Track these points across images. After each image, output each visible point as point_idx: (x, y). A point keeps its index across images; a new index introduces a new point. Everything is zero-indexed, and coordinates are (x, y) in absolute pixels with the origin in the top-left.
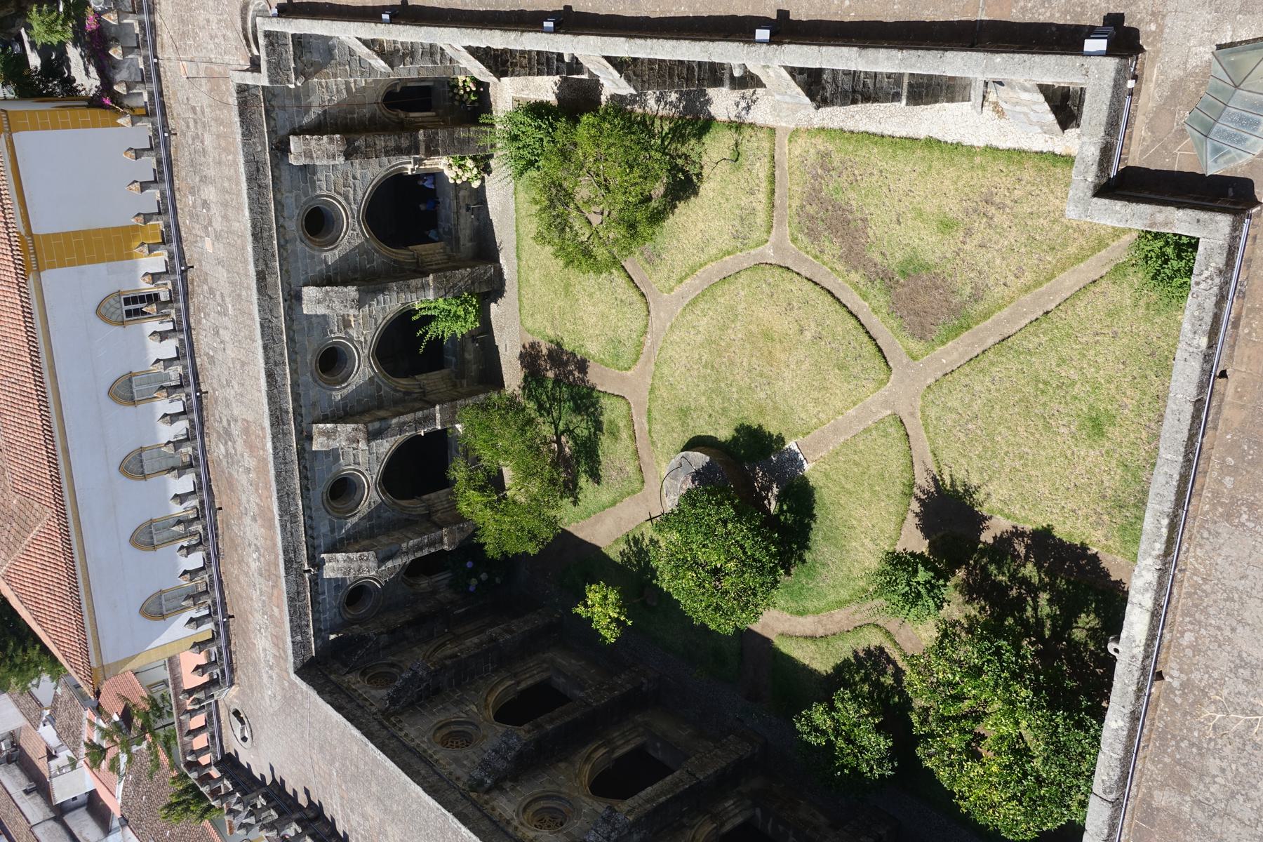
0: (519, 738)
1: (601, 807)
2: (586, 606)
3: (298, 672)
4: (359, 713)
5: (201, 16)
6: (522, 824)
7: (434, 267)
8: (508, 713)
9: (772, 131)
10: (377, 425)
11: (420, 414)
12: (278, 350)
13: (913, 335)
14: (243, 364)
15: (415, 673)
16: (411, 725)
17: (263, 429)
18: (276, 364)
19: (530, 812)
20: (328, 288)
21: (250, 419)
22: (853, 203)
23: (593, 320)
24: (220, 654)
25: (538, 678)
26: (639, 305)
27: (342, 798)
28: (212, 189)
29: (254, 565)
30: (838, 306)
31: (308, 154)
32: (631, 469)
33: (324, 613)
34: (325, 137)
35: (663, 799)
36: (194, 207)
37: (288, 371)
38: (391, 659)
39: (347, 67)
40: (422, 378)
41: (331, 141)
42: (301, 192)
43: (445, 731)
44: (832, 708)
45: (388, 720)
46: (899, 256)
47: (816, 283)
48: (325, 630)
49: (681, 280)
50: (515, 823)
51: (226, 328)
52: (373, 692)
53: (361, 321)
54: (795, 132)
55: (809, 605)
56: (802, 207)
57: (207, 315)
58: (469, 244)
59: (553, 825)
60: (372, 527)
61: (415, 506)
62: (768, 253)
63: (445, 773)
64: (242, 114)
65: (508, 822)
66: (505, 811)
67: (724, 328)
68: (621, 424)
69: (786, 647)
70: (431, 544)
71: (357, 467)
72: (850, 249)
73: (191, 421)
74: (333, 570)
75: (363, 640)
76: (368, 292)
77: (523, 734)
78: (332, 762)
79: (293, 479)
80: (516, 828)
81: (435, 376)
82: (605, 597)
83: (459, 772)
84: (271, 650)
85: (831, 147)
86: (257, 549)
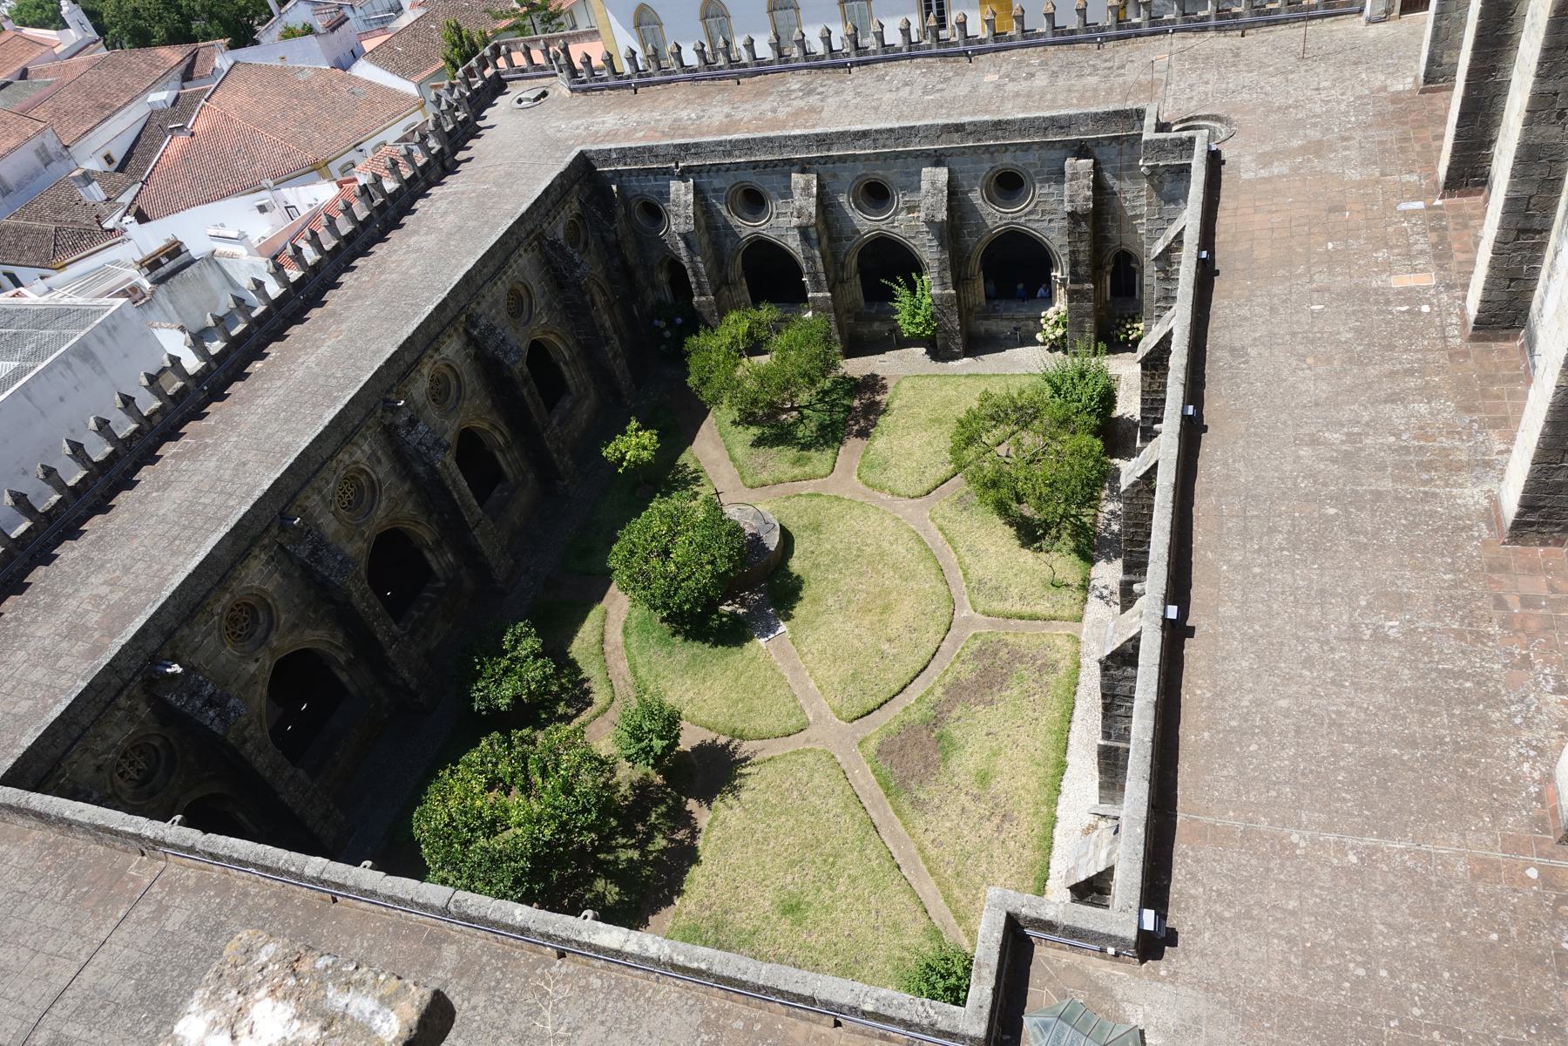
0: (515, 362)
1: (450, 437)
2: (638, 430)
3: (582, 153)
4: (542, 211)
5: (1211, 76)
6: (435, 363)
8: (538, 351)
9: (1079, 619)
10: (814, 236)
11: (823, 277)
12: (888, 142)
13: (882, 744)
15: (578, 266)
16: (529, 261)
17: (814, 126)
19: (446, 371)
20: (946, 192)
21: (824, 115)
22: (1009, 692)
24: (601, 80)
25: (570, 382)
26: (919, 489)
27: (463, 193)
28: (1045, 83)
29: (684, 114)
30: (912, 675)
31: (1075, 177)
32: (765, 476)
33: (638, 181)
36: (1028, 65)
41: (1087, 199)
43: (523, 292)
44: (537, 656)
45: (535, 239)
46: (957, 734)
47: (934, 655)
49: (941, 529)
50: (436, 357)
51: (911, 93)
52: (561, 226)
54: (1077, 641)
55: (633, 639)
56: (1006, 645)
57: (924, 75)
58: (982, 329)
60: (717, 228)
61: (736, 269)
62: (964, 612)
63: (484, 291)
64: (1116, 113)
65: (437, 350)
66: (448, 347)
67: (895, 567)
68: (807, 468)
69: (594, 616)
70: (699, 284)
71: (774, 216)
72: (965, 688)
73: (823, 57)
74: (677, 190)
75: (611, 217)
76: (941, 231)
77: (519, 367)
78: (496, 184)
80: (431, 357)
82: (645, 448)
83: (484, 305)
84: (603, 129)
85: (1061, 673)
86: (699, 118)
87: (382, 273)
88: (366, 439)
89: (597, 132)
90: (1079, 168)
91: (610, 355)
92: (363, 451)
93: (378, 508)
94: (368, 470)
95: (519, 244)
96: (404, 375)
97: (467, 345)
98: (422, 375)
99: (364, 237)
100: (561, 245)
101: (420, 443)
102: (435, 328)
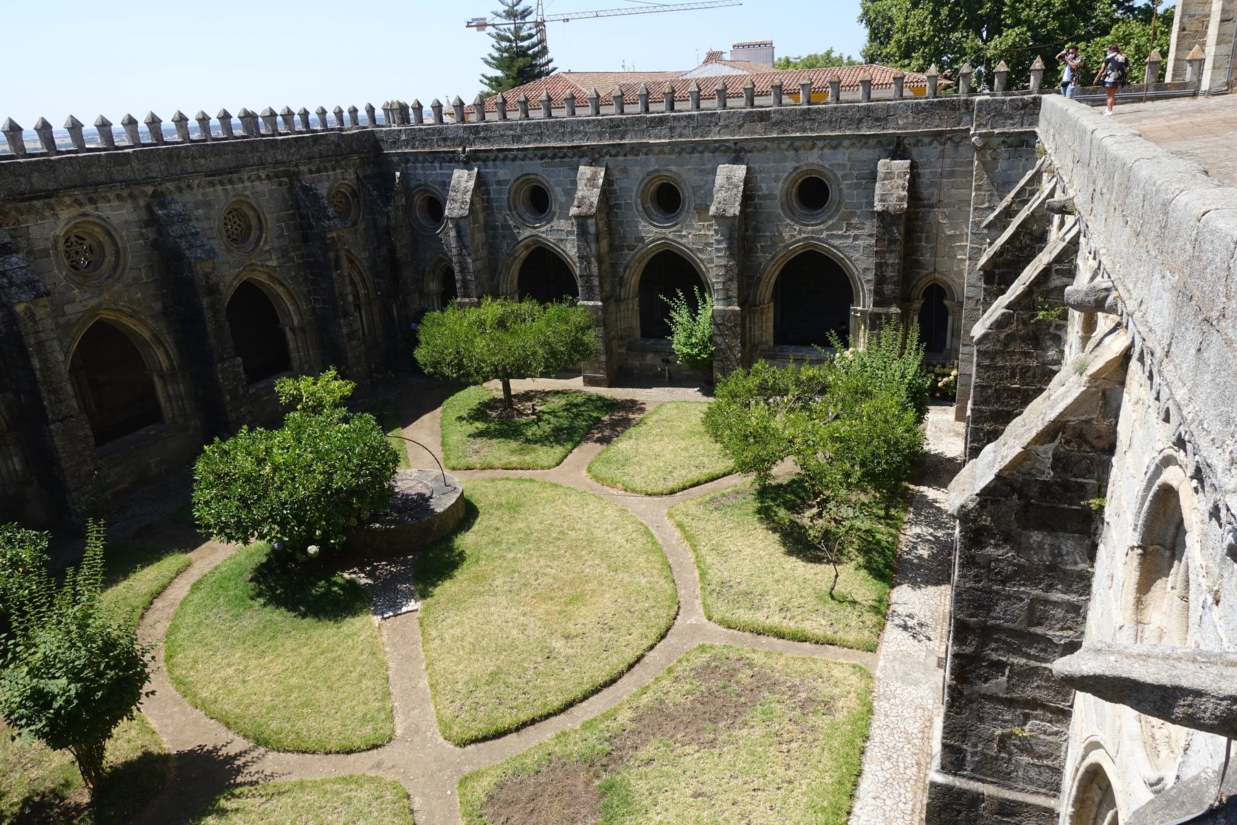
4: (304, 152)
9: (872, 649)
10: (592, 230)
11: (596, 282)
12: (686, 132)
13: (500, 786)
18: (672, 129)
20: (741, 188)
22: (745, 732)
25: (294, 355)
26: (661, 487)
30: (587, 687)
31: (889, 176)
32: (474, 460)
33: (423, 168)
34: (905, 193)
35: (36, 363)
37: (663, 141)
39: (986, 205)
40: (634, 304)
41: (901, 199)
42: (847, 171)
43: (254, 222)
46: (642, 786)
47: (631, 666)
48: (406, 168)
49: (680, 526)
53: (702, 233)
54: (866, 674)
56: (751, 665)
60: (495, 228)
62: (693, 617)
67: (604, 556)
68: (527, 458)
69: (171, 562)
70: (465, 283)
72: (670, 717)
74: (459, 177)
76: (731, 229)
79: (555, 141)
81: (635, 321)
85: (840, 716)
90: (894, 168)
91: (345, 331)
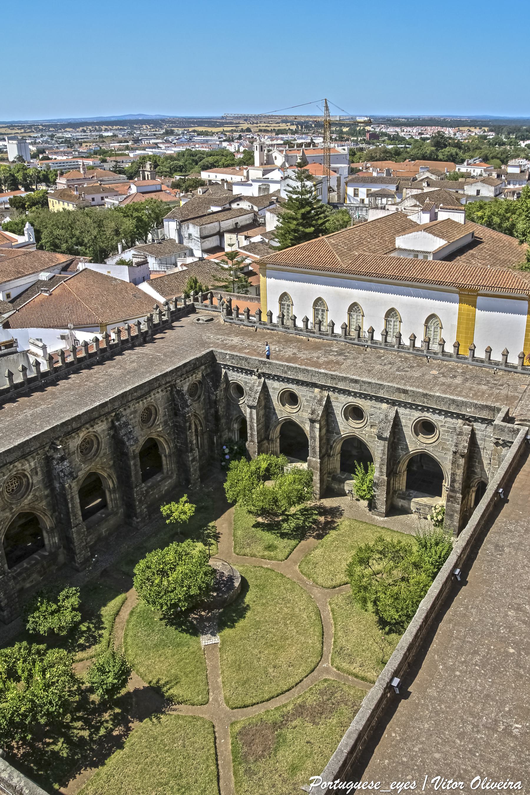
3: (212, 351)
4: (179, 374)
6: (89, 432)
7: (392, 481)
11: (318, 450)
14: (369, 371)
15: (188, 406)
16: (162, 396)
17: (334, 371)
19: (94, 438)
20: (392, 423)
21: (342, 366)
23: (333, 557)
27: (147, 354)
35: (70, 506)
36: (456, 371)
38: (202, 398)
43: (153, 411)
44: (74, 609)
45: (169, 386)
51: (391, 368)
52: (188, 384)
55: (134, 618)
57: (402, 361)
58: (400, 504)
59: (83, 447)
61: (276, 433)
63: (131, 404)
64: (487, 406)
65: (92, 426)
66: (99, 427)
71: (301, 410)
73: (354, 339)
75: (216, 386)
78: (165, 355)
81: (338, 465)
82: (185, 513)
83: (128, 411)
84: (230, 343)
86: (280, 351)
87: (86, 381)
88: (34, 459)
89: (226, 344)
92: (30, 465)
93: (26, 498)
94: (29, 476)
95: (160, 386)
96: (68, 434)
97: (110, 429)
98: (79, 436)
99: (88, 362)
100: (183, 394)
101: (62, 471)
102: (96, 414)
